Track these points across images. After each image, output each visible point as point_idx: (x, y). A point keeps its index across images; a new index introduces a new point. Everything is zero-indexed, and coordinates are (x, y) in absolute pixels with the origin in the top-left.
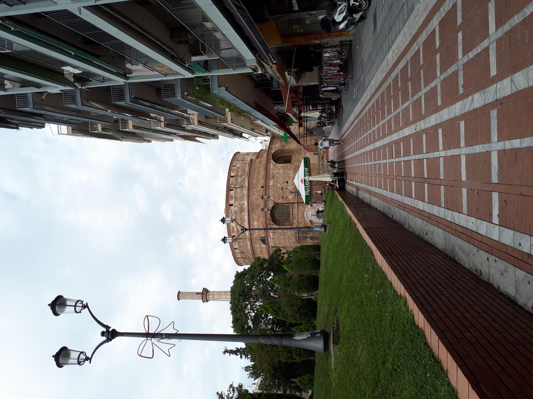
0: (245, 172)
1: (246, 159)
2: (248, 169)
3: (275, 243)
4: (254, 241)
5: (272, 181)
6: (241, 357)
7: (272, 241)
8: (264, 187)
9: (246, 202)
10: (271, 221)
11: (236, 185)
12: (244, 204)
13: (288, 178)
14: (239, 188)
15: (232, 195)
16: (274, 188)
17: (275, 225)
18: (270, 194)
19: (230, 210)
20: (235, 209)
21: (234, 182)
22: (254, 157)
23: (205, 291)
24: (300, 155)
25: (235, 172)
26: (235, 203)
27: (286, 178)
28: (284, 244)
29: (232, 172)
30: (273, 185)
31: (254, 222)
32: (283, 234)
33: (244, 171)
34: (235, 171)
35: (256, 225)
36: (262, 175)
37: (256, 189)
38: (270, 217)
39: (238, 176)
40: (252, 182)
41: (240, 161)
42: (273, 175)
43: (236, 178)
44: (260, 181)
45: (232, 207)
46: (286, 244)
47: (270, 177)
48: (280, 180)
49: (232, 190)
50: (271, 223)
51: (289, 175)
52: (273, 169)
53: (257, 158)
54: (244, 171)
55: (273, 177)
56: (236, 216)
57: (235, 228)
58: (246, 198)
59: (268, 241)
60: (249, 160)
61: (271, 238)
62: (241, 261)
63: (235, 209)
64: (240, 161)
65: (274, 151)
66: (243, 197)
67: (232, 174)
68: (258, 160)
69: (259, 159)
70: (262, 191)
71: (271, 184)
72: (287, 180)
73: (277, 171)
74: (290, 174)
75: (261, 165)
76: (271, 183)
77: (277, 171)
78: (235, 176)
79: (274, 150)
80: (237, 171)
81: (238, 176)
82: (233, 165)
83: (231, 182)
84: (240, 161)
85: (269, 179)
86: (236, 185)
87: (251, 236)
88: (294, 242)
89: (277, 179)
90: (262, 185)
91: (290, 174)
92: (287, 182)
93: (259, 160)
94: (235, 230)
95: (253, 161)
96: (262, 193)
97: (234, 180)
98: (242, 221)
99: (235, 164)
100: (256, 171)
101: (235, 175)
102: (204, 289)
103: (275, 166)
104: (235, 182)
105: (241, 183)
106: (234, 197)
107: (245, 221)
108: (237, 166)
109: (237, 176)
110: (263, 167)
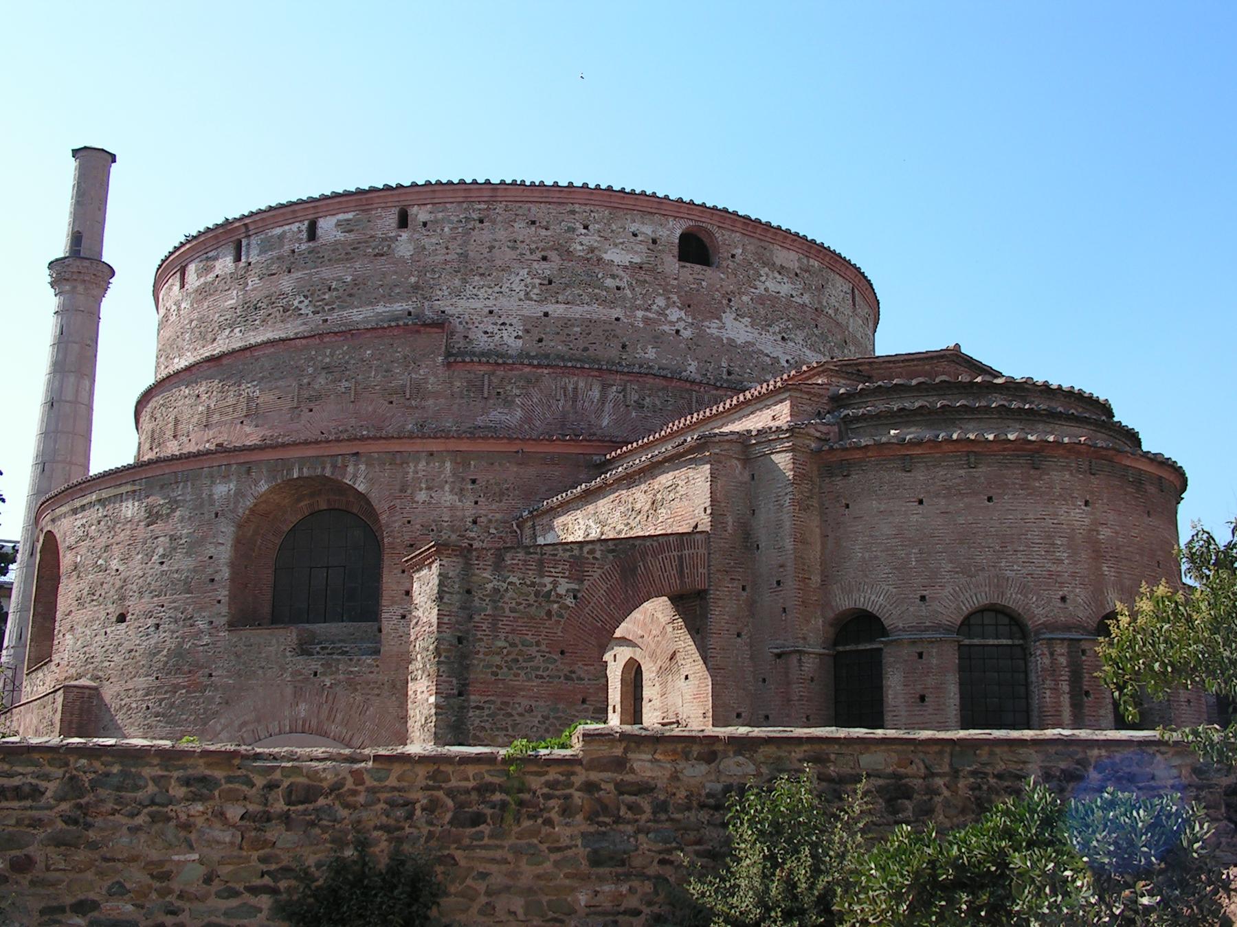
0: (343, 308)
24: (289, 690)
25: (340, 236)
29: (350, 216)
33: (353, 293)
45: (176, 288)
49: (238, 259)
52: (202, 505)
65: (361, 488)
67: (332, 221)
74: (157, 626)
79: (371, 481)
82: (415, 209)
83: (278, 231)
84: (466, 243)
92: (122, 618)
110: (353, 421)
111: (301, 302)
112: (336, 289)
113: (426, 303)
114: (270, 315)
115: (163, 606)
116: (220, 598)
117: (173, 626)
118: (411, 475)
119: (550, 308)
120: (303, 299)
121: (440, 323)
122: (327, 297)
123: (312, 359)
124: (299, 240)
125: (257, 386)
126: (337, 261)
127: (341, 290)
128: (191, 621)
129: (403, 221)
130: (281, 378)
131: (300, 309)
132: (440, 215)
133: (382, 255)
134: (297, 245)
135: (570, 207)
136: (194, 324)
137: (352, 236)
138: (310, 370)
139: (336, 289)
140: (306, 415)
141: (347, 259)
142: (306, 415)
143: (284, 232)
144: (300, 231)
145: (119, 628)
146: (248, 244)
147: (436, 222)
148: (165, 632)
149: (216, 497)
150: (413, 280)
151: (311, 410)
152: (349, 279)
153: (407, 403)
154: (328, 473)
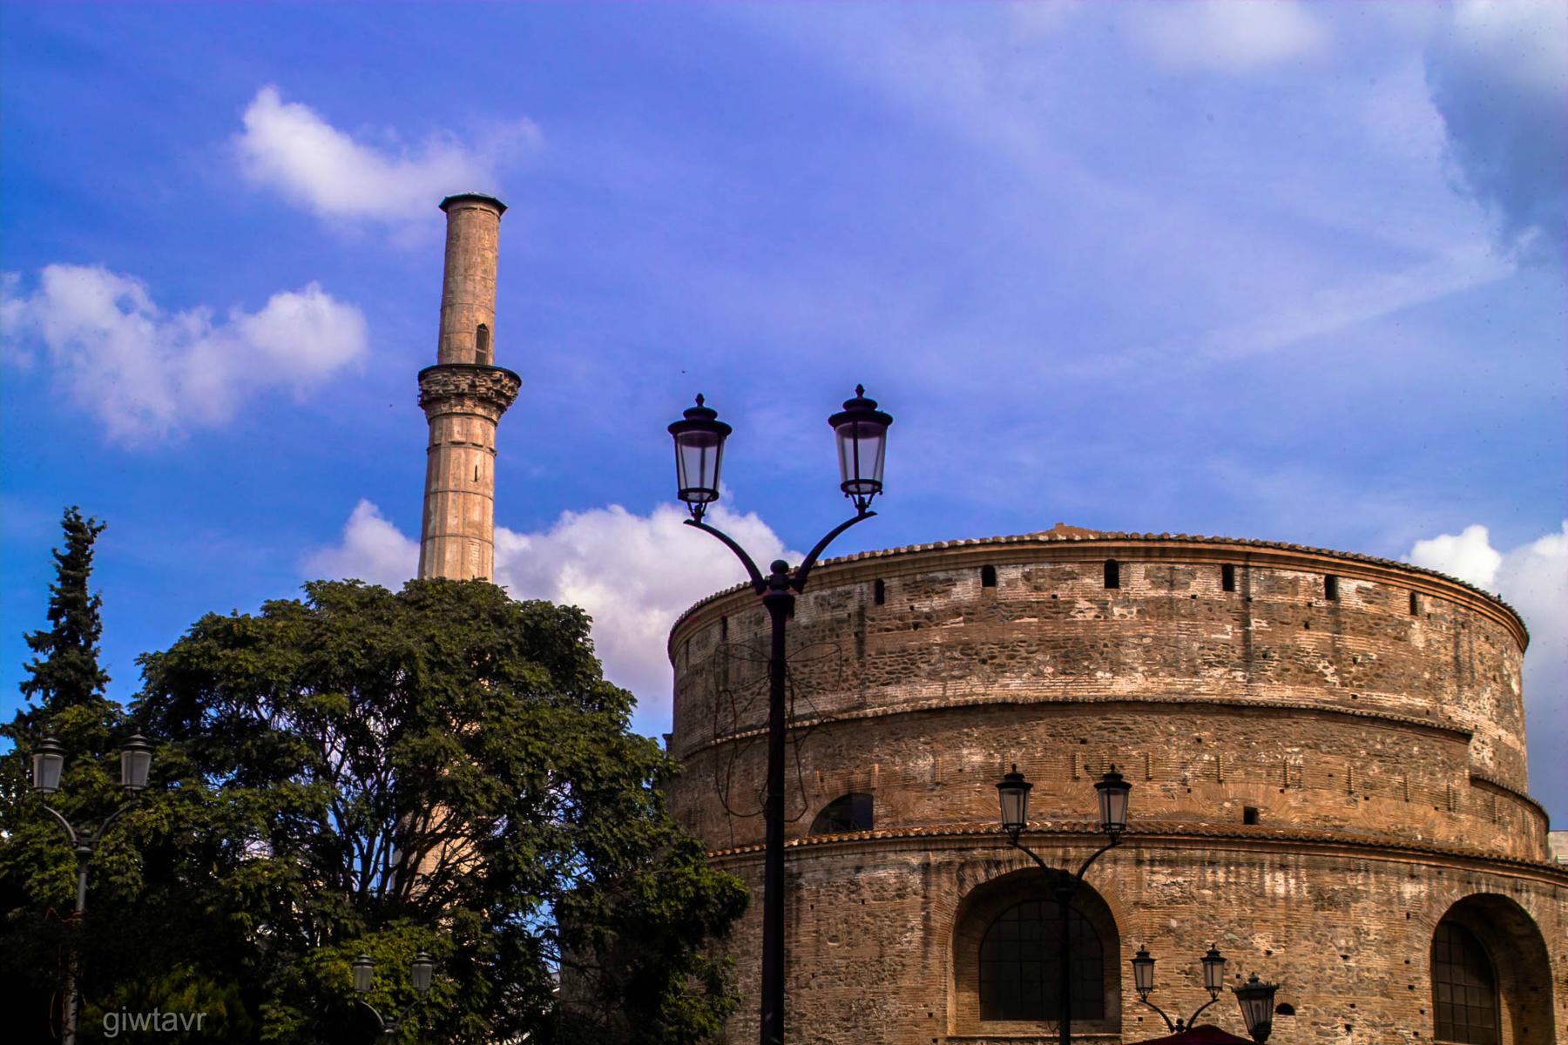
0: (1372, 688)
1: (1468, 693)
2: (1392, 709)
4: (844, 741)
5: (1298, 888)
6: (37, 643)
8: (1243, 829)
9: (1133, 687)
10: (987, 871)
11: (1269, 612)
12: (1117, 668)
13: (1316, 1014)
14: (1246, 637)
15: (1188, 583)
16: (1241, 904)
17: (952, 902)
18: (1193, 873)
19: (1076, 568)
20: (1082, 604)
21: (1287, 599)
22: (1487, 753)
23: (498, 387)
25: (1361, 605)
26: (1127, 603)
27: (1315, 998)
28: (811, 968)
29: (1369, 585)
30: (1262, 895)
31: (982, 743)
32: (887, 959)
33: (1379, 674)
34: (1372, 609)
35: (960, 757)
36: (1348, 811)
37: (1235, 767)
38: (1017, 867)
39: (1338, 628)
40: (1285, 735)
41: (1450, 646)
42: (1340, 898)
43: (1324, 618)
44: (1293, 798)
45: (1094, 581)
46: (813, 983)
47: (1328, 879)
48: (1304, 956)
49: (1228, 585)
50: (968, 871)
51: (1340, 1021)
53: (1478, 780)
54: (1379, 674)
55: (1323, 900)
56: (1027, 608)
57: (937, 602)
58: (1162, 687)
59: (841, 846)
60: (1463, 715)
61: (858, 869)
62: (705, 646)
63: (1082, 604)
64: (1457, 646)
65: (1533, 915)
66: (1172, 666)
68: (1460, 784)
69: (1471, 797)
70: (1215, 811)
71: (1268, 878)
72: (1300, 1010)
73: (1374, 926)
74: (1348, 1028)
75: (1420, 811)
76: (1278, 884)
77: (1374, 926)
78: (1334, 611)
79: (1540, 910)
80: (1371, 627)
81: (1338, 628)
83: (1289, 575)
84: (1457, 646)
85: (1312, 867)
86: (1269, 612)
87: (879, 719)
89: (1307, 930)
90: (1262, 816)
91: (1348, 1028)
93: (1464, 791)
94: (924, 606)
95: (1456, 747)
96: (1201, 810)
97: (1301, 599)
98: (993, 658)
99: (1428, 608)
100: (1375, 769)
101: (1343, 604)
102: (513, 376)
103: (1417, 917)
104: (1294, 607)
105: (1284, 648)
106: (1178, 594)
107: (988, 681)
108: (1417, 625)
109: (1338, 623)
110: (1408, 821)
111: (1325, 667)
112: (1361, 664)
113: (1438, 705)
114: (1288, 670)
115: (1353, 1006)
116: (1424, 1008)
117: (1368, 1030)
118: (1562, 909)
119: (1502, 732)
120: (1327, 664)
121: (1464, 736)
122: (1353, 669)
123: (1363, 740)
124: (1317, 594)
125: (1298, 753)
126: (1361, 632)
127: (1368, 666)
128: (1393, 1028)
129: (1414, 608)
130: (1329, 753)
131: (1326, 676)
132: (1439, 610)
133: (1400, 639)
134: (1314, 599)
135: (1500, 628)
136: (1147, 641)
137: (1372, 609)
138: (1363, 752)
139: (1361, 664)
140: (1362, 804)
141: (1370, 634)
142: (1362, 804)
143: (1296, 579)
144: (1316, 583)
145: (1283, 1020)
146: (1245, 576)
147: (1435, 616)
148: (1361, 1035)
149: (1407, 896)
150: (1427, 676)
151: (1367, 799)
152: (1375, 657)
153: (1449, 813)
154: (1508, 894)
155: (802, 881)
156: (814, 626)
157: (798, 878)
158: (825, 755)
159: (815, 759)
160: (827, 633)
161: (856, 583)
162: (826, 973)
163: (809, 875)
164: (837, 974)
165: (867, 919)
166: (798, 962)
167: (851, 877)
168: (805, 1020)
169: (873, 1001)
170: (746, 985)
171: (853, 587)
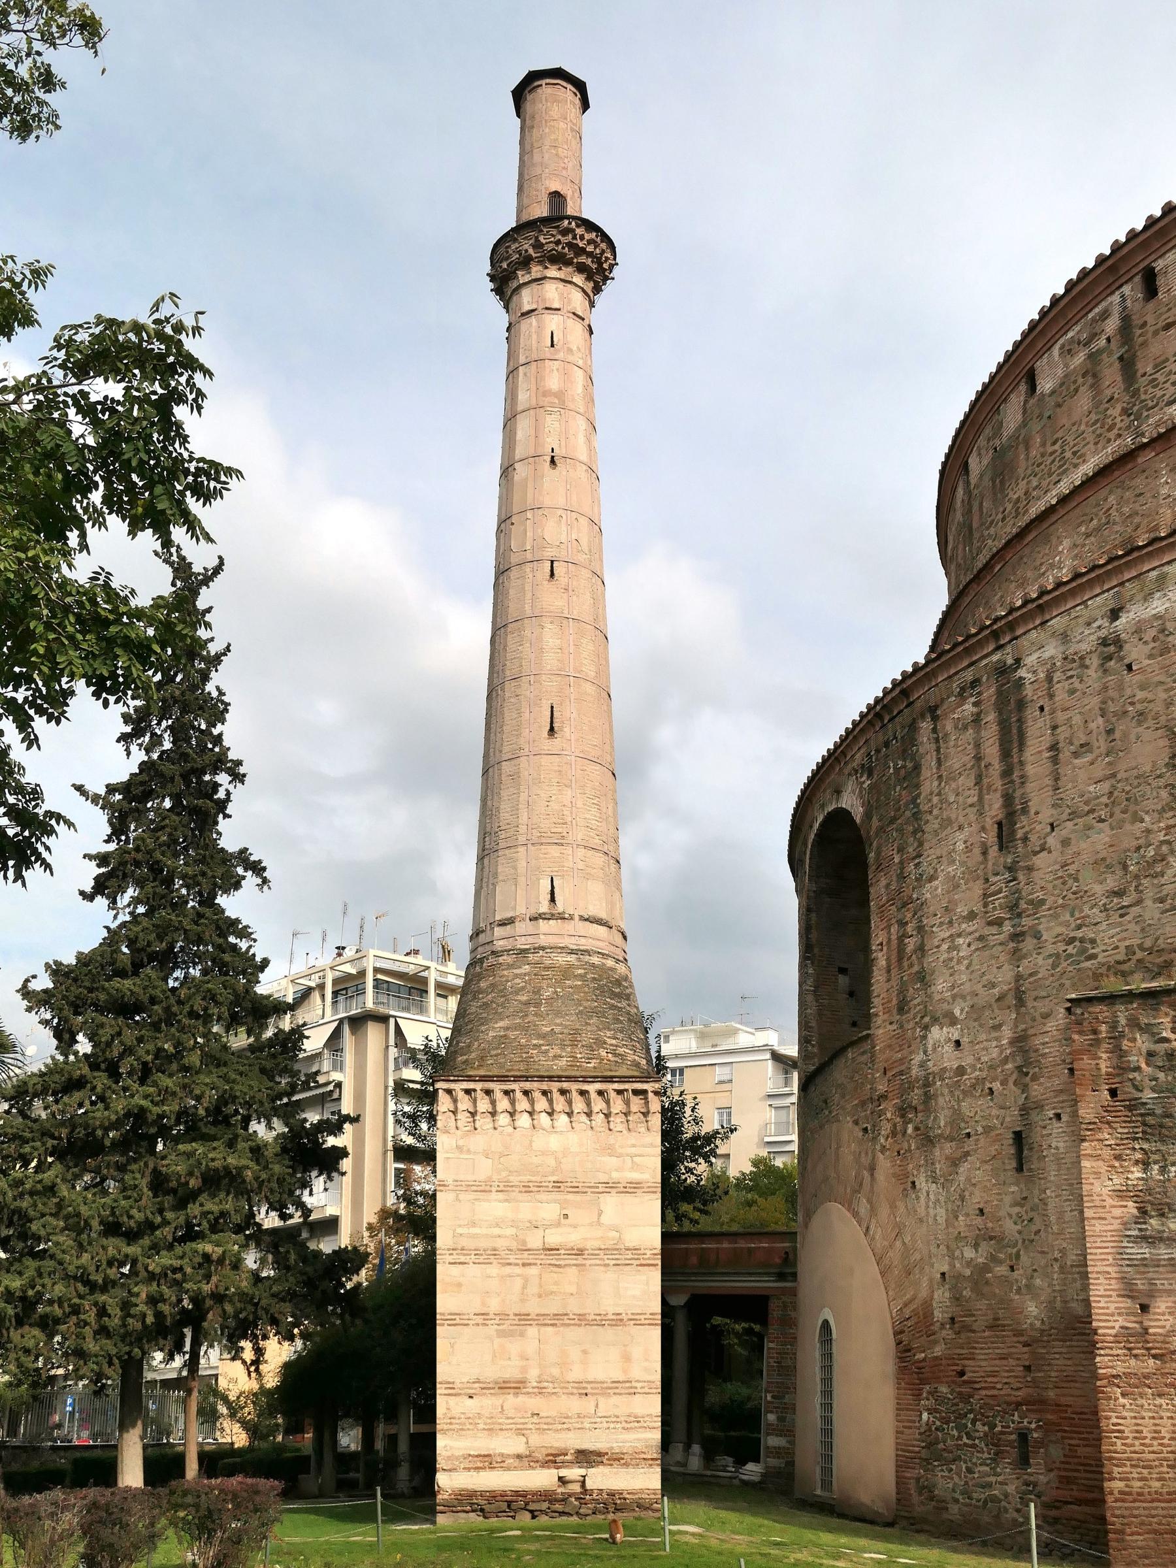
3: (1060, 690)
7: (1085, 647)
28: (1047, 815)
46: (1051, 841)
61: (1115, 614)
88: (1085, 953)
155: (1022, 673)
156: (1062, 384)
157: (1016, 670)
158: (1088, 535)
159: (1075, 546)
160: (1080, 380)
161: (1112, 293)
162: (1074, 815)
163: (1031, 660)
164: (1092, 811)
165: (1140, 695)
166: (1025, 811)
167: (1103, 633)
168: (1043, 911)
169: (1169, 843)
170: (951, 879)
171: (1110, 299)
